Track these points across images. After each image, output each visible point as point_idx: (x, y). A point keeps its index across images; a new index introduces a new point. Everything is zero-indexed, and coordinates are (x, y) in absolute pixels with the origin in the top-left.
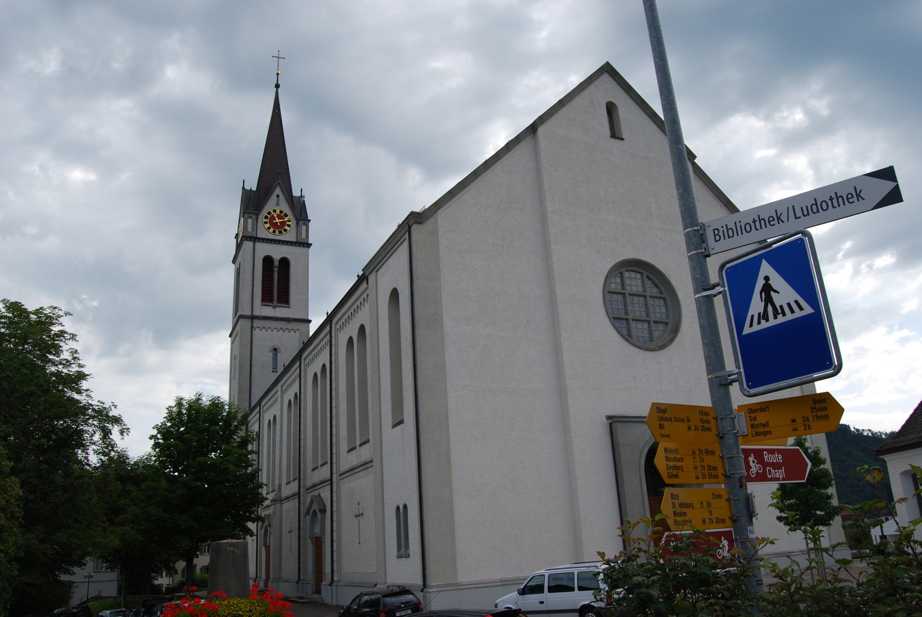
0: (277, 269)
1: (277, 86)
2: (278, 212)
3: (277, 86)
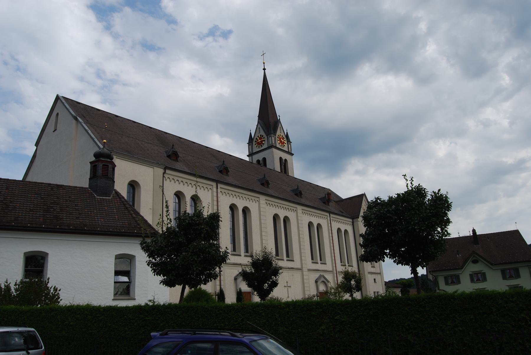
0: (283, 164)
1: (264, 69)
2: (281, 136)
3: (264, 69)
